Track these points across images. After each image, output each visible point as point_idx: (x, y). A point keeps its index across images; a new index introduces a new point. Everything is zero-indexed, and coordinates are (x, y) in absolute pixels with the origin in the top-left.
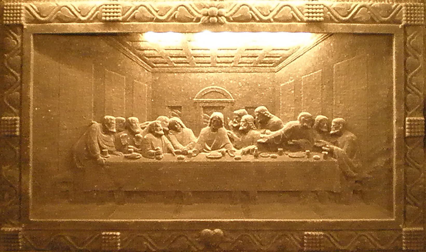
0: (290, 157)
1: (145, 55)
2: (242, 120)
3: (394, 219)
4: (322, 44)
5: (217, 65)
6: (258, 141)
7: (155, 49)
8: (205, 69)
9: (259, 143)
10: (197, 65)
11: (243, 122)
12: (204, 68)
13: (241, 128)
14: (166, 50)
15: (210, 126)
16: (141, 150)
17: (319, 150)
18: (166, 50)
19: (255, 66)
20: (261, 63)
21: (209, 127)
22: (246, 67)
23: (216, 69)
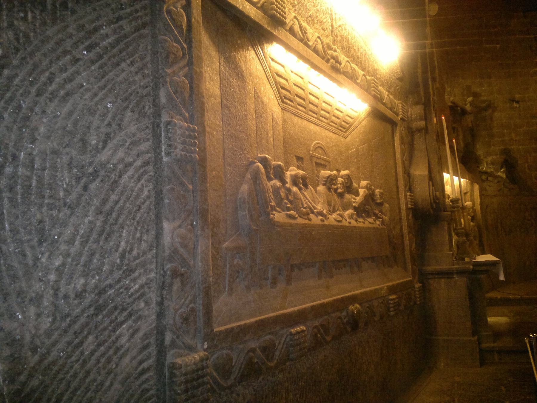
0: (369, 222)
1: (280, 83)
2: (338, 183)
3: (410, 279)
4: (366, 120)
5: (321, 118)
6: (354, 205)
7: (288, 79)
8: (314, 120)
9: (355, 208)
10: (310, 113)
11: (341, 184)
12: (314, 119)
13: (339, 191)
14: (295, 85)
15: (324, 185)
16: (294, 208)
17: (378, 217)
18: (295, 85)
19: (337, 128)
20: (341, 126)
21: (324, 187)
22: (334, 127)
23: (319, 122)
